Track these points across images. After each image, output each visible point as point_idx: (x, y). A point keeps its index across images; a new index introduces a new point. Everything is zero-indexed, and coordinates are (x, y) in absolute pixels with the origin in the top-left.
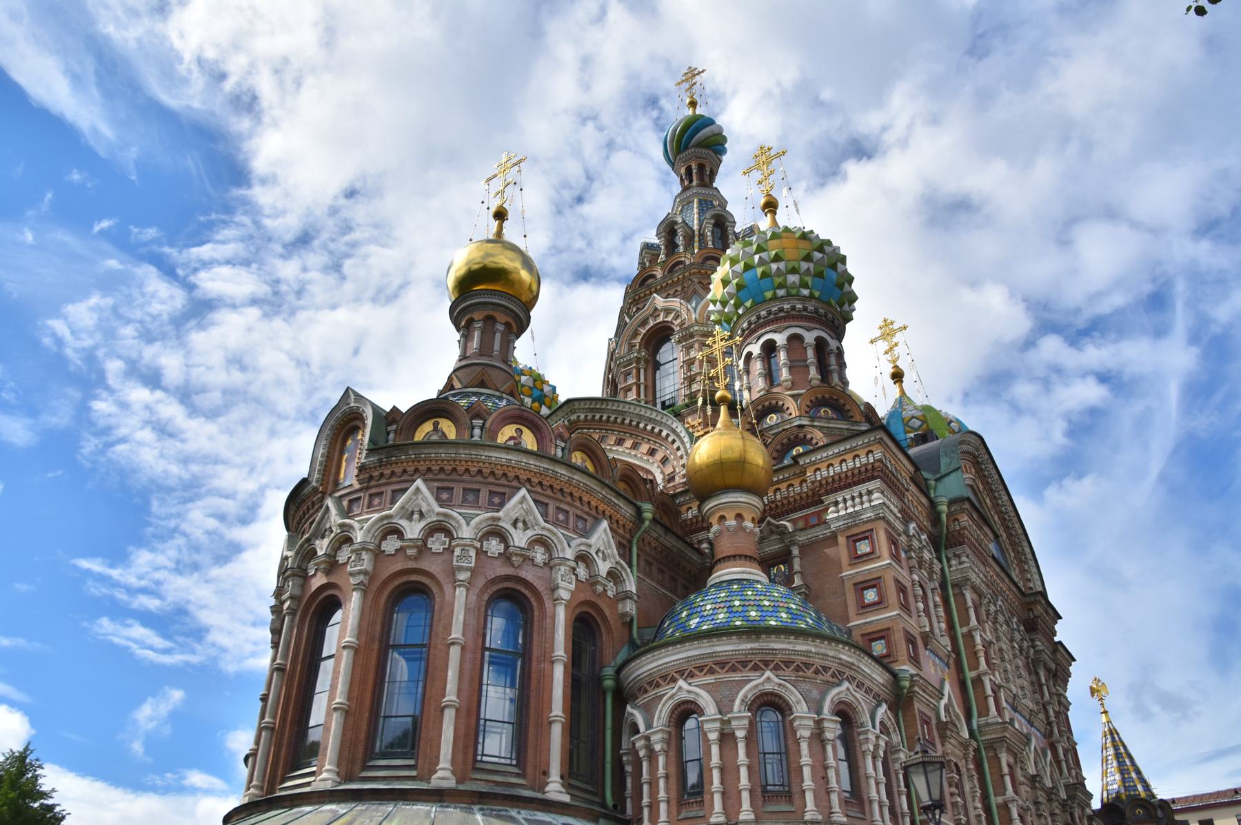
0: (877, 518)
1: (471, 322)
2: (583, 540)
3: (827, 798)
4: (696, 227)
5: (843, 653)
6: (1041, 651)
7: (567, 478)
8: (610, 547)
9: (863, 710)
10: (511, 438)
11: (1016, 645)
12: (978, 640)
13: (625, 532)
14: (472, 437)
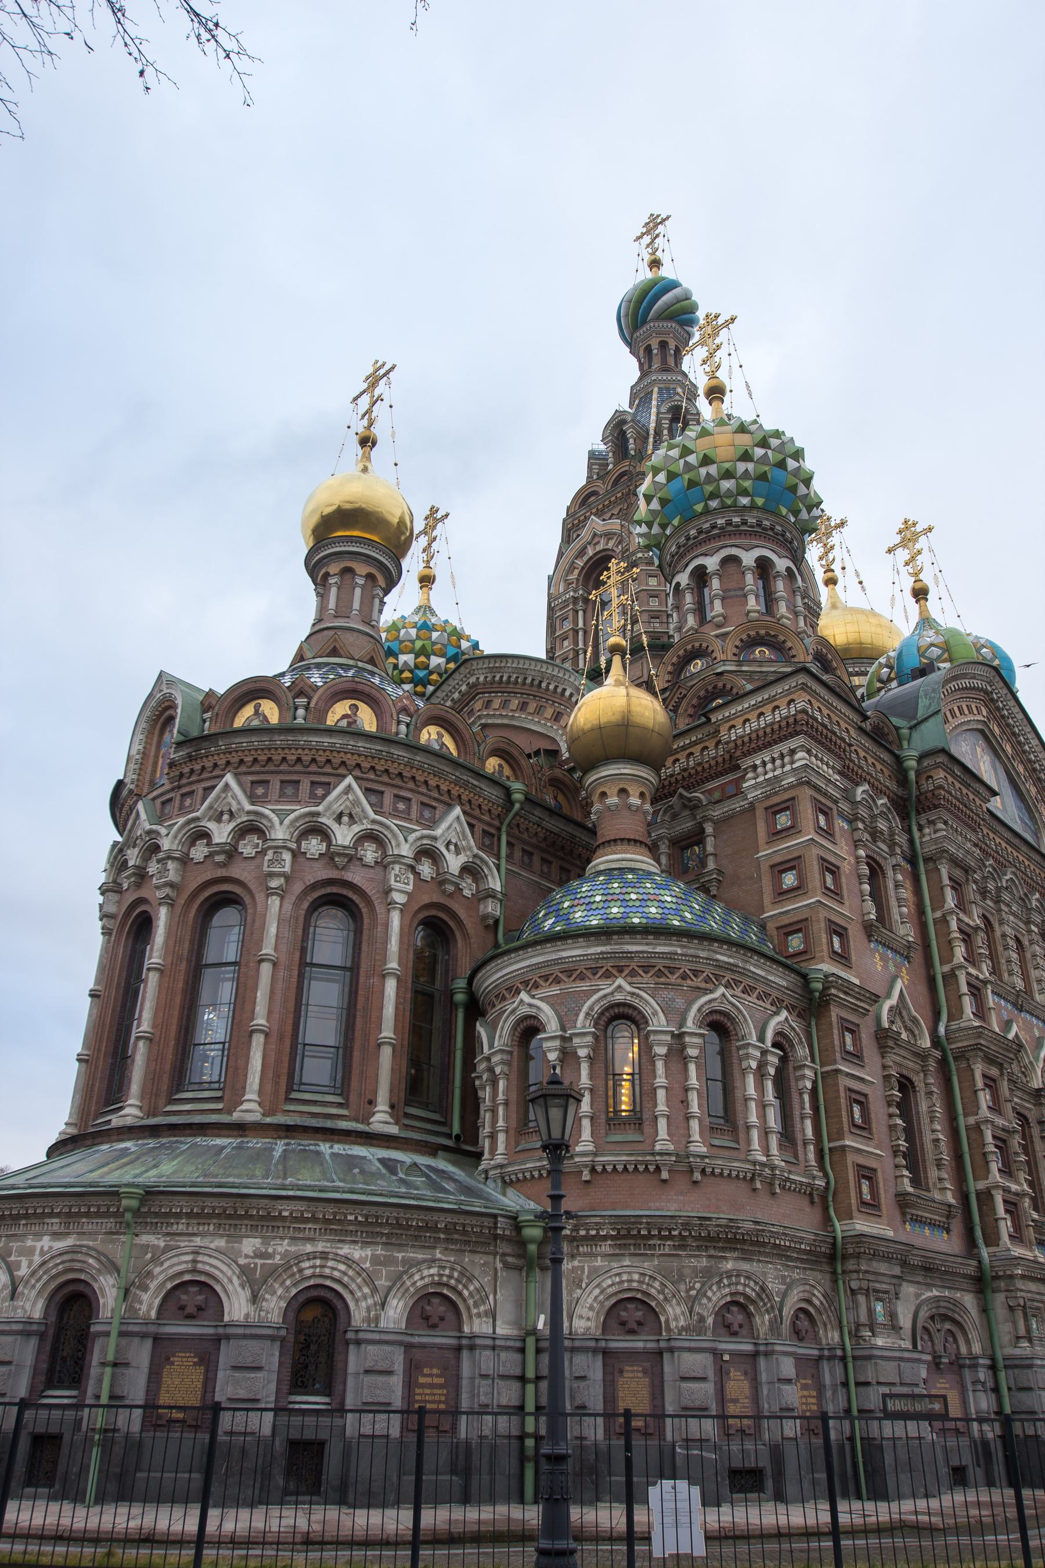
0: (800, 783)
1: (327, 575)
2: (426, 832)
4: (653, 425)
5: (721, 954)
8: (465, 838)
9: (746, 1020)
10: (344, 717)
11: (1033, 927)
12: (954, 925)
13: (492, 819)
14: (295, 719)
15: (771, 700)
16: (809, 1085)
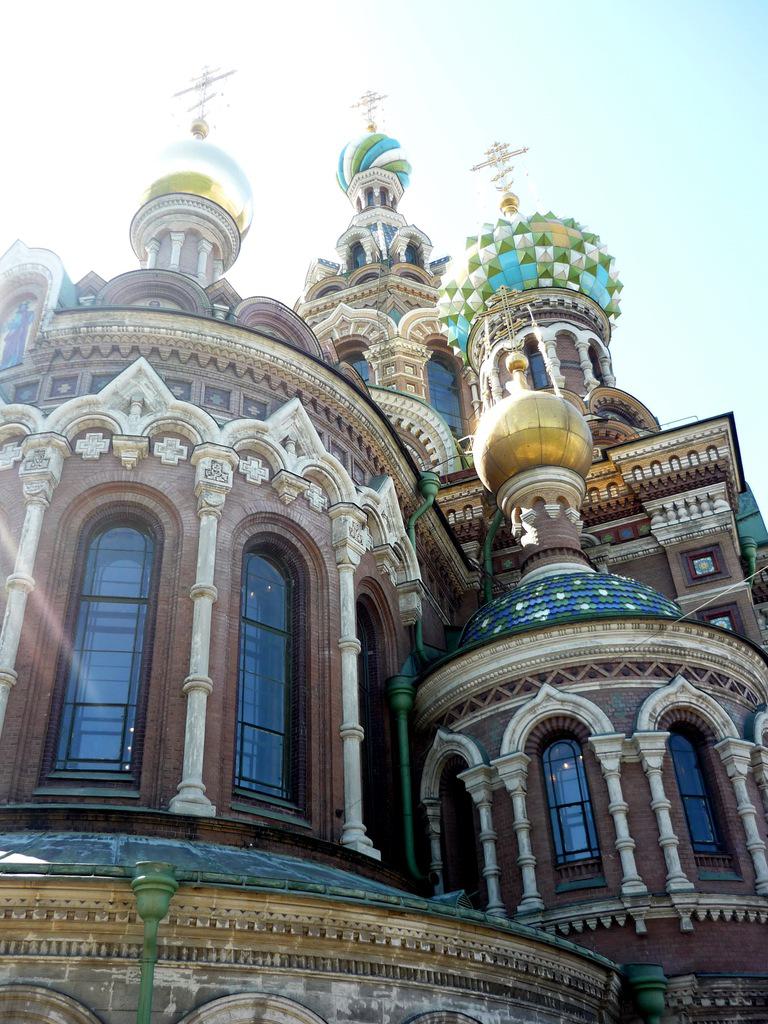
7: (347, 404)
15: (688, 442)
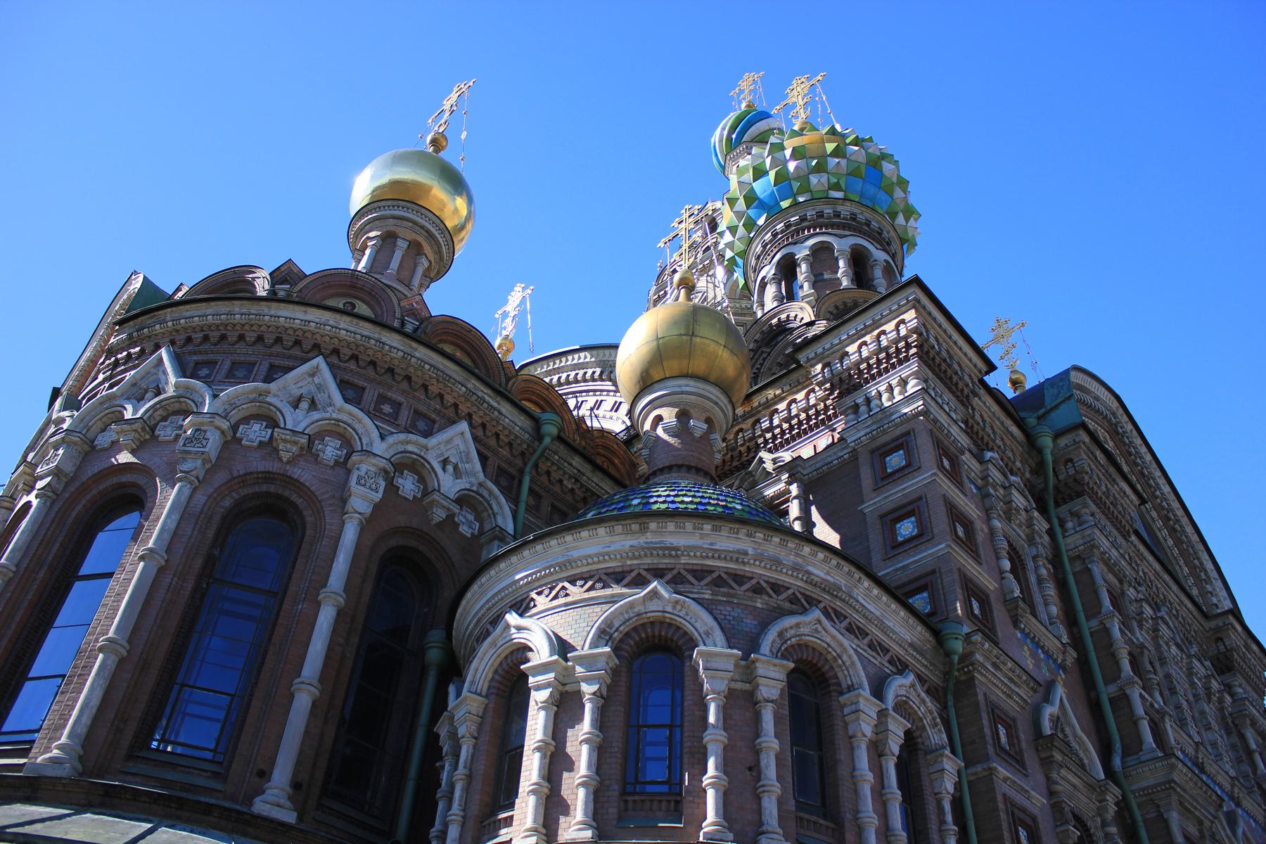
3: (755, 806)
5: (814, 565)
6: (1243, 699)
9: (853, 663)
13: (512, 455)
16: (950, 786)
